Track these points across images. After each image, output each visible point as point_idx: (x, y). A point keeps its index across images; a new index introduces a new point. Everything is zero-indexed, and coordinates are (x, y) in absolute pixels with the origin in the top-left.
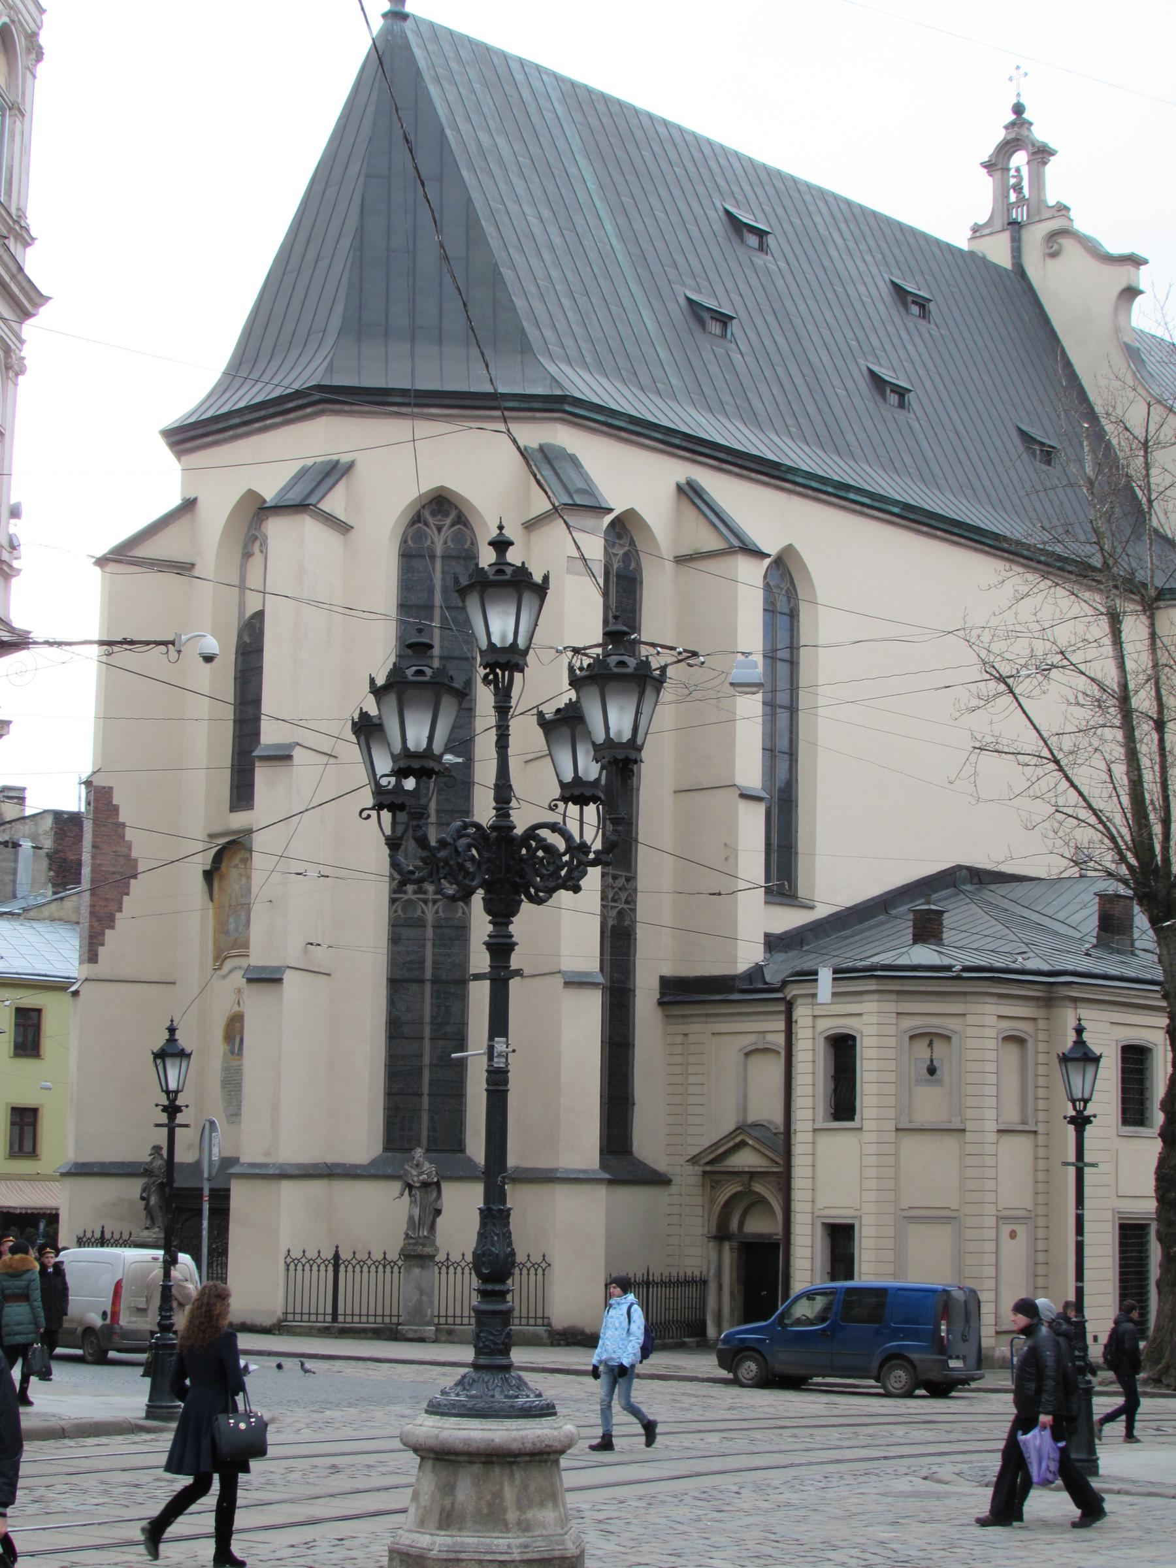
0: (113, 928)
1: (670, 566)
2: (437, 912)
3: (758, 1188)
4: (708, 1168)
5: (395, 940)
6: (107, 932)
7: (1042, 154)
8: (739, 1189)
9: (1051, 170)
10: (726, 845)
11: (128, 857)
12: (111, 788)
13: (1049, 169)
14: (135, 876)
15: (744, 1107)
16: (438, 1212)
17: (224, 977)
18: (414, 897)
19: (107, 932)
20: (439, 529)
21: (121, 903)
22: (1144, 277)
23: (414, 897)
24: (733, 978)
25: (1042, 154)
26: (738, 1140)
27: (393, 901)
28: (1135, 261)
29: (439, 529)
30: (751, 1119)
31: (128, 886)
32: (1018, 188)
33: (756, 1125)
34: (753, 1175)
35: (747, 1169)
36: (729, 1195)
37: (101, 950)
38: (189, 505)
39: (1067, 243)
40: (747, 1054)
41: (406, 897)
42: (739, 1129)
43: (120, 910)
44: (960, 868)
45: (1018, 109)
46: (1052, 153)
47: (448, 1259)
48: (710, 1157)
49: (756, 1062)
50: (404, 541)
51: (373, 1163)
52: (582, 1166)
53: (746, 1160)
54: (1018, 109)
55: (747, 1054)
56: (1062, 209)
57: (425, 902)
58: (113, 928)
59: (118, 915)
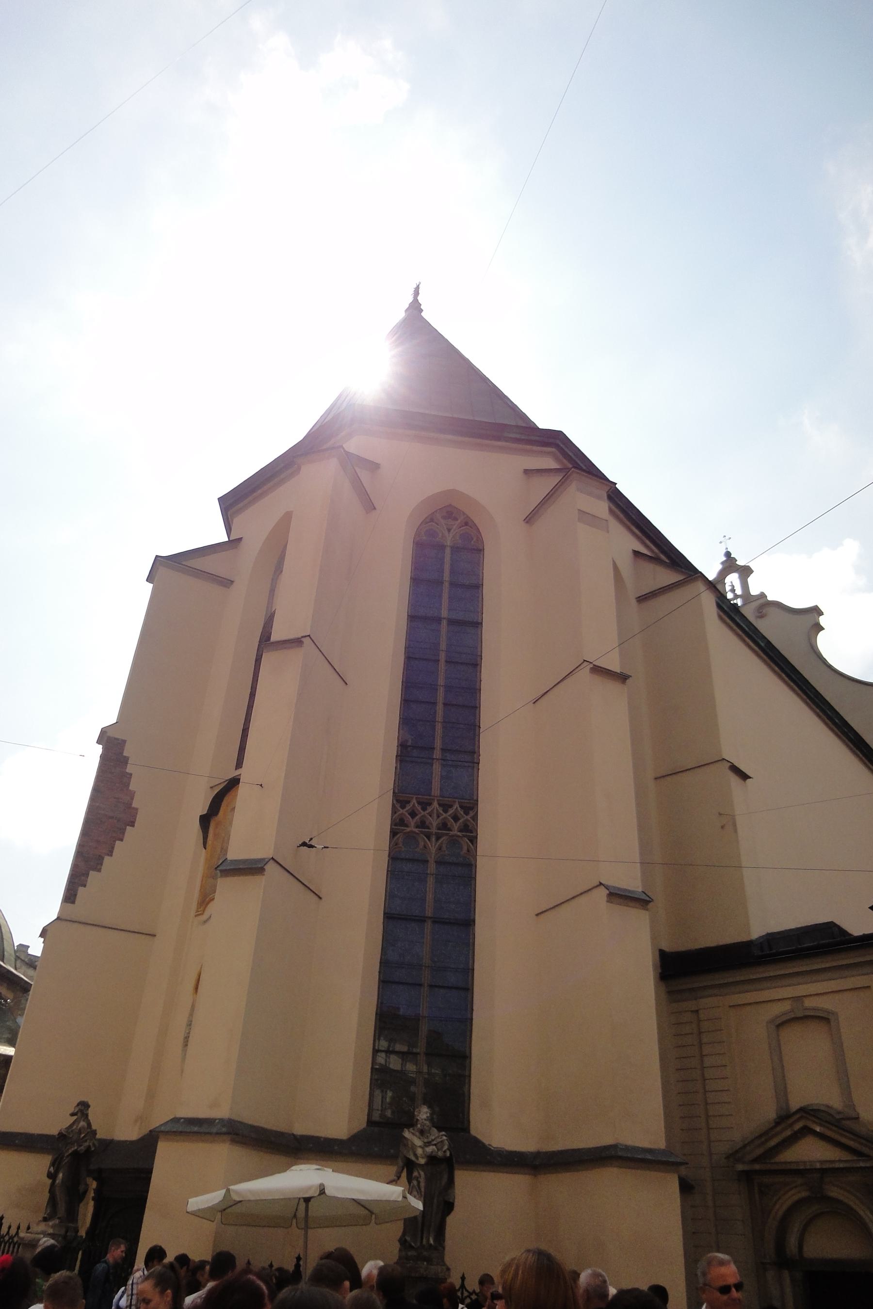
0: (99, 870)
1: (634, 602)
2: (440, 848)
3: (834, 1192)
4: (757, 1167)
5: (393, 874)
6: (92, 873)
7: (745, 572)
8: (804, 1194)
9: (750, 580)
10: (720, 814)
11: (129, 806)
12: (124, 742)
13: (749, 580)
14: (132, 824)
15: (781, 1091)
16: (449, 1207)
17: (205, 922)
18: (416, 830)
19: (92, 873)
20: (449, 530)
21: (113, 848)
22: (822, 620)
23: (416, 830)
24: (749, 944)
25: (745, 572)
26: (798, 1126)
27: (393, 833)
28: (816, 611)
29: (449, 530)
30: (795, 1104)
31: (123, 832)
32: (733, 590)
33: (806, 1112)
34: (825, 1172)
35: (818, 1166)
36: (789, 1203)
37: (81, 890)
38: (233, 543)
39: (771, 610)
40: (778, 1026)
41: (408, 829)
42: (784, 1118)
43: (110, 853)
44: (832, 922)
45: (728, 554)
46: (752, 572)
47: (463, 1286)
48: (759, 1151)
49: (792, 1036)
50: (418, 534)
51: (355, 1139)
52: (646, 1144)
53: (811, 1152)
54: (728, 554)
55: (778, 1026)
56: (763, 595)
57: (429, 838)
58: (99, 870)
59: (107, 860)
